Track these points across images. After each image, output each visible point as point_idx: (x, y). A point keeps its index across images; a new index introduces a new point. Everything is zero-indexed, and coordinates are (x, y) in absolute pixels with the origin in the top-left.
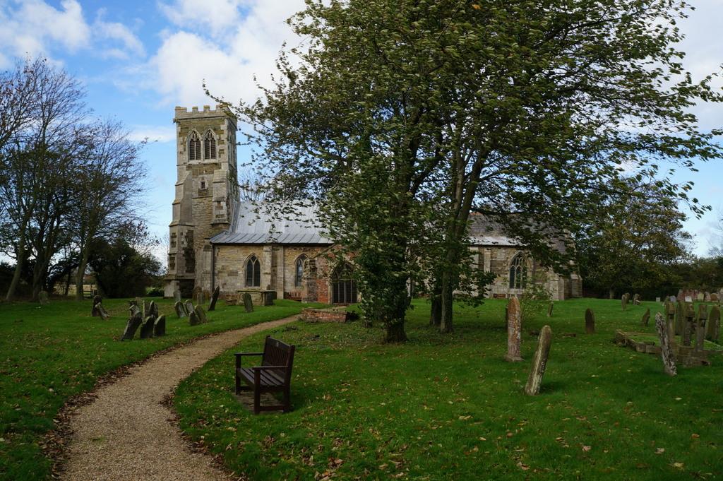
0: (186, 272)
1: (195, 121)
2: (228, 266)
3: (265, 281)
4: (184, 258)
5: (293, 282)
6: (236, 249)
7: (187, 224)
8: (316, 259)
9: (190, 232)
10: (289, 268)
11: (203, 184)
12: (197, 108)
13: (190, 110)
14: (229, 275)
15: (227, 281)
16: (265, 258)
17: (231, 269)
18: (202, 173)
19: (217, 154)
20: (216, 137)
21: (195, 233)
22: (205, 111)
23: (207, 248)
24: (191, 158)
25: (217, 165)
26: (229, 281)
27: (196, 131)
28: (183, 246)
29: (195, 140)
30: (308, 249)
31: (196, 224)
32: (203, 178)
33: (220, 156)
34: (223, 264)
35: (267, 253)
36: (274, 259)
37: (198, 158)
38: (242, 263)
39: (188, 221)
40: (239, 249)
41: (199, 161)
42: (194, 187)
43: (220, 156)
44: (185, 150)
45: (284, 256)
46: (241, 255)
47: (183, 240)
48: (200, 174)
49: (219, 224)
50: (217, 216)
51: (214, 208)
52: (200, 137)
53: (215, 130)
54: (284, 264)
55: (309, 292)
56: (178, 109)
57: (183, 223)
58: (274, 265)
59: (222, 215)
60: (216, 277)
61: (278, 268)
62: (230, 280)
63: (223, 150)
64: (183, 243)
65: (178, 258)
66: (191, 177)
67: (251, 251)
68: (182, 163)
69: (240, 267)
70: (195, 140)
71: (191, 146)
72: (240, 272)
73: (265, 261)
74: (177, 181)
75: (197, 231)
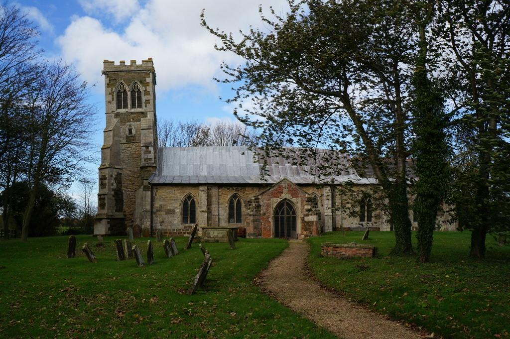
0: (116, 211)
1: (123, 74)
2: (165, 205)
3: (201, 219)
4: (114, 198)
5: (226, 219)
6: (173, 189)
7: (116, 167)
8: (260, 197)
9: (119, 175)
10: (223, 206)
11: (130, 130)
12: (124, 62)
13: (117, 63)
14: (166, 214)
15: (165, 219)
16: (201, 197)
17: (168, 208)
18: (129, 121)
19: (143, 104)
20: (142, 89)
21: (122, 175)
22: (131, 65)
23: (146, 188)
24: (119, 107)
25: (144, 114)
26: (167, 219)
27: (123, 82)
28: (112, 187)
29: (122, 90)
30: (240, 188)
31: (125, 167)
32: (130, 126)
33: (146, 106)
34: (161, 203)
35: (203, 192)
36: (209, 198)
37: (126, 107)
38: (179, 202)
39: (117, 165)
40: (176, 189)
41: (127, 110)
42: (122, 134)
43: (146, 106)
44: (113, 99)
45: (218, 195)
47: (112, 182)
48: (128, 122)
49: (147, 167)
50: (145, 160)
51: (142, 152)
52: (127, 88)
53: (141, 82)
54: (218, 202)
55: (255, 228)
56: (106, 62)
57: (113, 166)
58: (209, 204)
59: (150, 159)
60: (154, 215)
61: (213, 206)
62: (168, 218)
63: (149, 100)
64: (112, 184)
65: (108, 198)
66: (119, 124)
67: (188, 191)
68: (110, 111)
69: (177, 205)
70: (122, 90)
71: (119, 96)
72: (177, 211)
73: (201, 200)
74: (105, 127)
75: (125, 174)
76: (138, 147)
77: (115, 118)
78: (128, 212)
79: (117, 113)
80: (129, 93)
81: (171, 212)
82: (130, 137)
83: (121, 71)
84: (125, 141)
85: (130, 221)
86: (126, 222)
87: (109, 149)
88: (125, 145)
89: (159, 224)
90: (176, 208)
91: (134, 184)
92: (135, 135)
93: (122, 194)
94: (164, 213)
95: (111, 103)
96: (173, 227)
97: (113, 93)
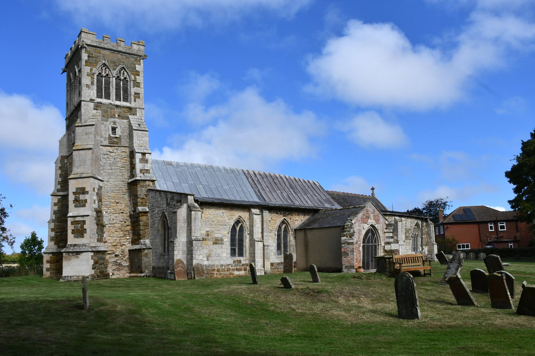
0: (98, 241)
1: (107, 52)
2: (212, 232)
9: (100, 188)
11: (114, 129)
18: (113, 116)
31: (106, 179)
33: (135, 100)
34: (208, 229)
37: (108, 97)
40: (224, 211)
41: (109, 101)
43: (135, 100)
44: (92, 83)
46: (227, 218)
48: (112, 117)
66: (100, 118)
67: (237, 214)
71: (99, 82)
76: (123, 154)
77: (94, 109)
78: (111, 243)
79: (98, 103)
80: (113, 81)
81: (218, 242)
82: (113, 138)
83: (105, 49)
84: (106, 143)
85: (113, 255)
86: (107, 257)
87: (91, 151)
88: (107, 148)
89: (205, 259)
90: (224, 236)
91: (118, 203)
92: (120, 136)
93: (102, 215)
94: (212, 243)
95: (89, 88)
96: (222, 262)
97: (94, 74)
